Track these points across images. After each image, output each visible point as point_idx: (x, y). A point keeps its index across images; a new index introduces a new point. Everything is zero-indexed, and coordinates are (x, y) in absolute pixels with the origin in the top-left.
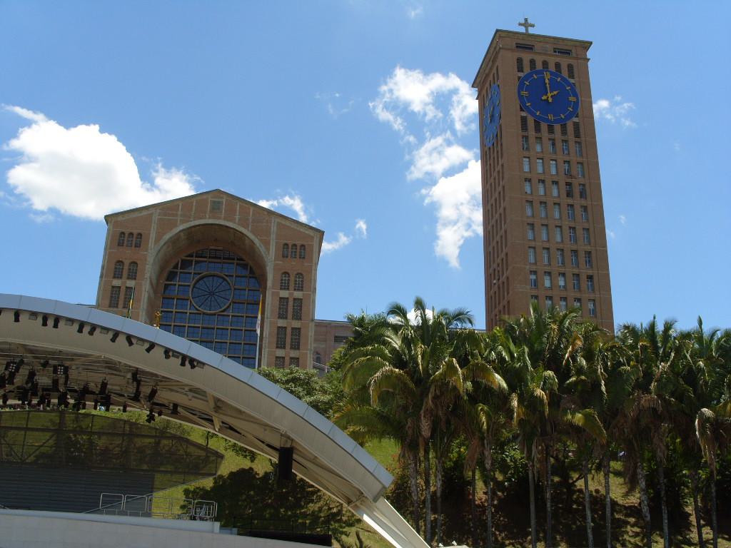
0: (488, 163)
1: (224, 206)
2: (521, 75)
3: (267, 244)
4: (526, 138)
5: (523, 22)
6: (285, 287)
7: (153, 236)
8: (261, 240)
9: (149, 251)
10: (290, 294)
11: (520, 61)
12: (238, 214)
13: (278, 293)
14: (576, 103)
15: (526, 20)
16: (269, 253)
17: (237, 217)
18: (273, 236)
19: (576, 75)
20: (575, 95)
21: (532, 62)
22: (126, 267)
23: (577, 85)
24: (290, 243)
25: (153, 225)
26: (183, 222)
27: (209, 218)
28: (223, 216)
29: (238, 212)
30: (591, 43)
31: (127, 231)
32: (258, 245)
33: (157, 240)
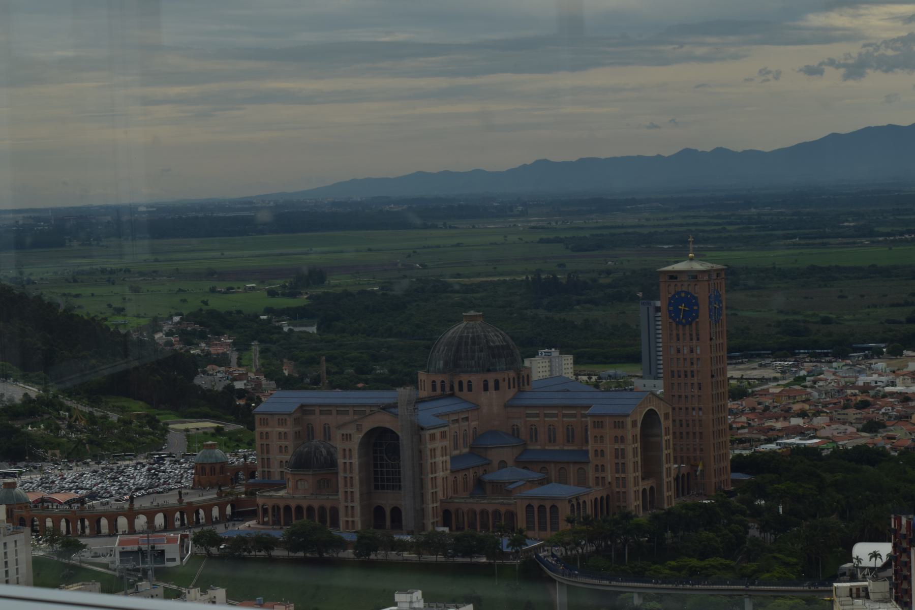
0: (674, 332)
33: (640, 418)
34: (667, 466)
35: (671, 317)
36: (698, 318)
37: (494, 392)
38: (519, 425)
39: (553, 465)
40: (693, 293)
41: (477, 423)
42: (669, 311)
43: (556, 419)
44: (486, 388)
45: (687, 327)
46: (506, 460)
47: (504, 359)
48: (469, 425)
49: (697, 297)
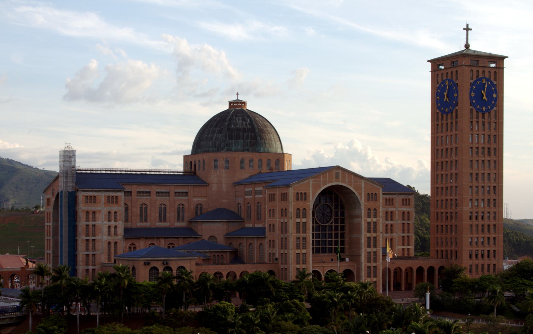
1: (341, 175)
2: (472, 81)
3: (360, 194)
4: (472, 122)
5: (465, 27)
6: (369, 216)
7: (311, 193)
8: (358, 192)
9: (311, 202)
10: (371, 220)
11: (472, 71)
12: (347, 178)
13: (367, 220)
14: (496, 98)
15: (467, 25)
16: (362, 200)
17: (347, 180)
18: (363, 190)
19: (497, 80)
20: (496, 93)
21: (478, 71)
22: (301, 212)
23: (498, 85)
24: (370, 193)
25: (310, 188)
26: (324, 185)
27: (335, 182)
28: (341, 180)
29: (347, 177)
30: (507, 57)
31: (299, 192)
32: (357, 195)
33: (313, 196)
34: (369, 250)
35: (438, 108)
36: (457, 106)
37: (224, 170)
38: (241, 203)
39: (245, 240)
40: (454, 80)
41: (205, 200)
42: (437, 101)
43: (261, 196)
44: (216, 167)
45: (449, 115)
46: (215, 236)
47: (242, 141)
48: (188, 199)
49: (457, 84)
